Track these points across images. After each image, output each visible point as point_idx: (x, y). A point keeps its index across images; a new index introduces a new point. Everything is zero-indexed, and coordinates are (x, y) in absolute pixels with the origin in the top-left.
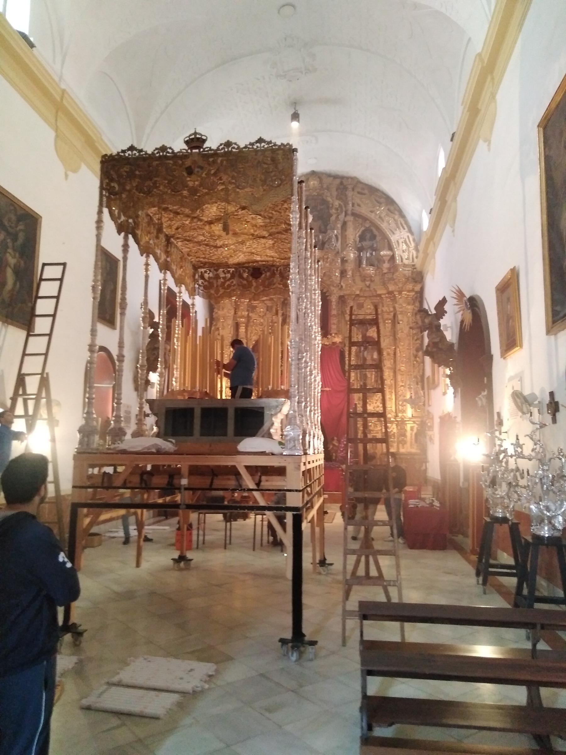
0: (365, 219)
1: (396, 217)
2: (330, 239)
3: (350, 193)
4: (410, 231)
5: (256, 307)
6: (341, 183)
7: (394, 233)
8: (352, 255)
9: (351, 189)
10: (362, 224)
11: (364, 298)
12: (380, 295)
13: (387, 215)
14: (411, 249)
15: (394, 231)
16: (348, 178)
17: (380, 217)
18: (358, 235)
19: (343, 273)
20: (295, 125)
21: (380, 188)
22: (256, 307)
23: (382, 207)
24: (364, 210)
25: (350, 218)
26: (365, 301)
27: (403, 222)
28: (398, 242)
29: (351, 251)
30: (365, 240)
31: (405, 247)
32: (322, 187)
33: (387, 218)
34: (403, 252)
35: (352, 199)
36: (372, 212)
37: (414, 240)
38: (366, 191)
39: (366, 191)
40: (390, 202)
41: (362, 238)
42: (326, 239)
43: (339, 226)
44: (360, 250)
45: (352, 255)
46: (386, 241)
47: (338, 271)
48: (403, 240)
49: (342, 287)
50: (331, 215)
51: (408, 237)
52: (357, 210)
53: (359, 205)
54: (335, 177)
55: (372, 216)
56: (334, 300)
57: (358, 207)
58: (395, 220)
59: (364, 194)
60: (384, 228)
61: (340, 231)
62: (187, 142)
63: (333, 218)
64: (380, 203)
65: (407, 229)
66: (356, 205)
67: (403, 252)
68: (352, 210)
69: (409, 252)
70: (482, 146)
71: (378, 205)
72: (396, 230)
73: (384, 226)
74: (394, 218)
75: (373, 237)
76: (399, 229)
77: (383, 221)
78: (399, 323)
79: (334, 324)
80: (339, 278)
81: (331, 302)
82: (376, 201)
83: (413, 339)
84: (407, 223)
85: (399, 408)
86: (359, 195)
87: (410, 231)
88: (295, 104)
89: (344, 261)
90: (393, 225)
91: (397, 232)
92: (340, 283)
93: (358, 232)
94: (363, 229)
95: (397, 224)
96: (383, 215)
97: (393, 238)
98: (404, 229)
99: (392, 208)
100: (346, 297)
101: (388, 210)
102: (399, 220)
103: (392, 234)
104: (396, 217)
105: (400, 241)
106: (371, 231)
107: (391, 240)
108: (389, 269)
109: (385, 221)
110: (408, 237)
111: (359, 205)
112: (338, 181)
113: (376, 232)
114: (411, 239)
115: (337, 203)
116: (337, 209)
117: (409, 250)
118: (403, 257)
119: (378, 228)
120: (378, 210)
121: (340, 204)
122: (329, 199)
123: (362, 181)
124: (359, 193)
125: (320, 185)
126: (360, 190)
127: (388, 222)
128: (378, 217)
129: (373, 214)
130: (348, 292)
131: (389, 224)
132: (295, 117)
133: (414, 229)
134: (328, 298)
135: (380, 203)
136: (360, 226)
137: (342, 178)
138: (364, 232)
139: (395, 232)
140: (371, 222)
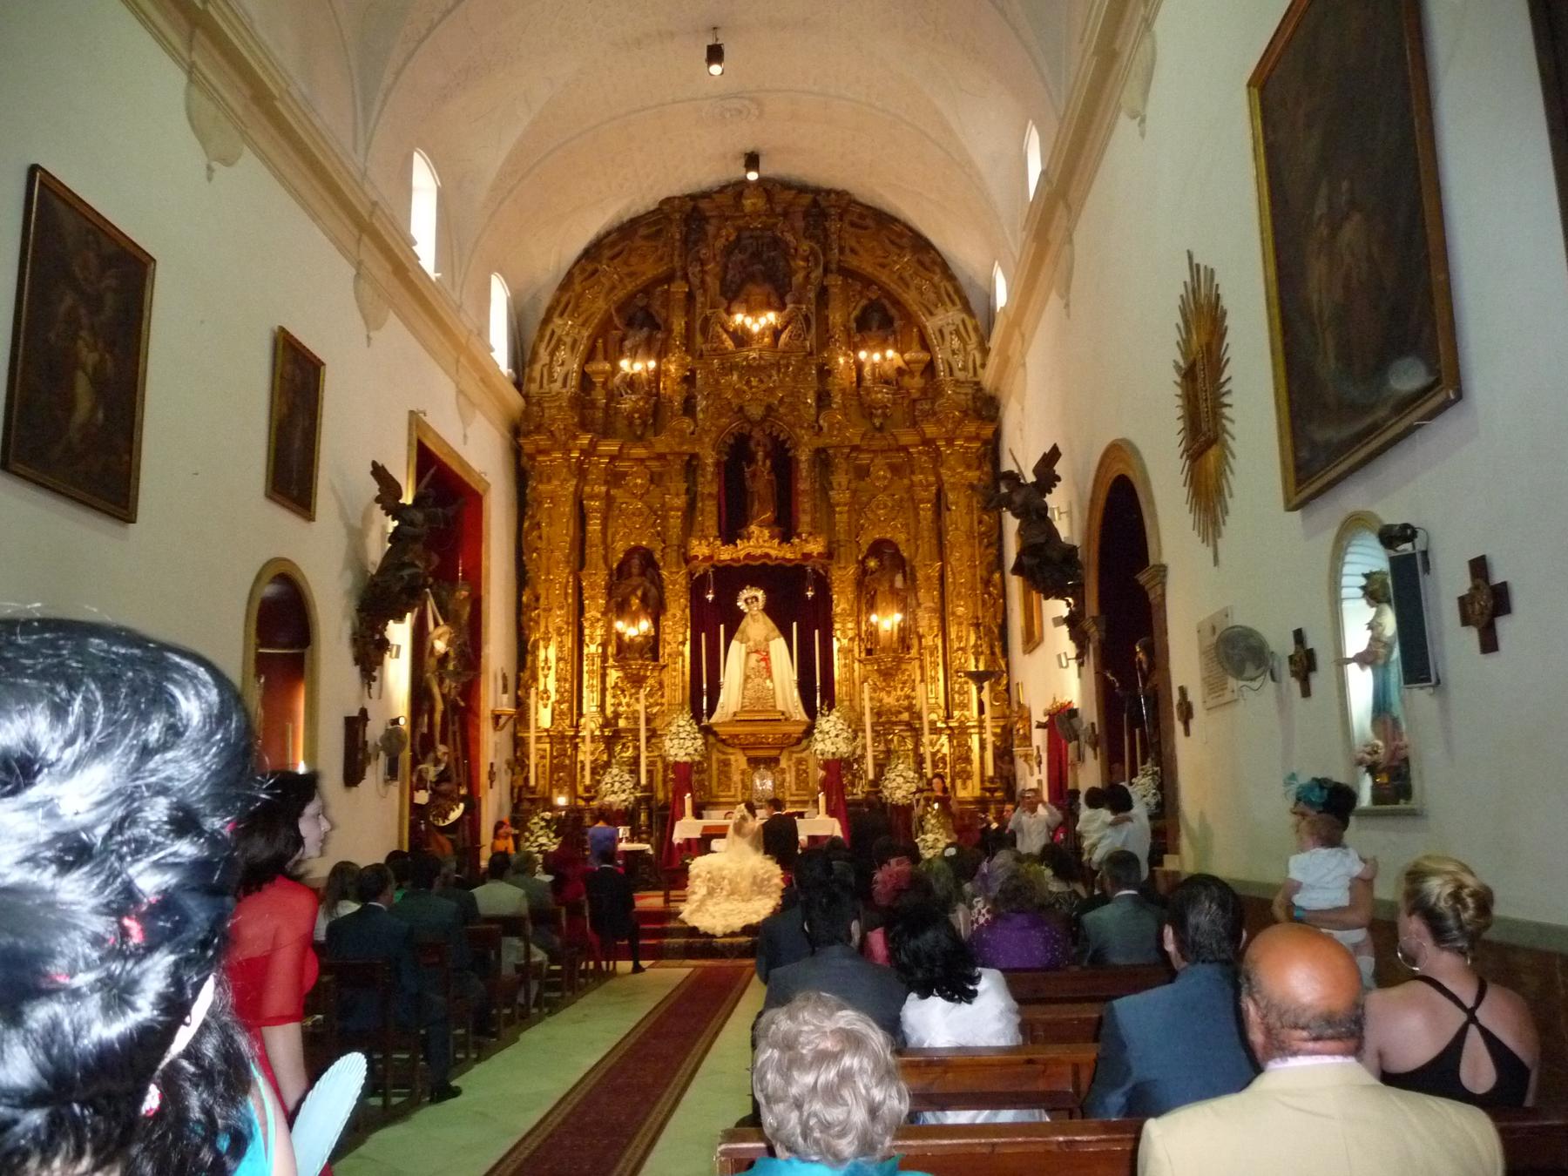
0: (868, 282)
1: (936, 279)
3: (833, 226)
4: (967, 308)
5: (625, 474)
6: (815, 203)
10: (861, 293)
11: (871, 455)
12: (905, 448)
13: (916, 273)
14: (969, 348)
15: (932, 309)
16: (829, 192)
17: (901, 278)
18: (852, 316)
19: (823, 399)
20: (716, 69)
21: (901, 217)
22: (625, 474)
24: (866, 265)
25: (835, 281)
26: (872, 460)
28: (941, 331)
31: (956, 343)
32: (772, 209)
33: (917, 281)
34: (954, 353)
35: (840, 237)
36: (883, 266)
37: (976, 329)
38: (869, 222)
40: (921, 245)
43: (812, 295)
48: (952, 328)
49: (821, 428)
51: (963, 321)
52: (853, 262)
53: (853, 250)
54: (802, 189)
55: (884, 277)
56: (803, 458)
58: (934, 285)
59: (866, 228)
61: (813, 308)
64: (902, 248)
65: (959, 306)
66: (847, 251)
67: (954, 353)
68: (840, 261)
69: (966, 353)
70: (1125, 127)
72: (936, 306)
73: (910, 298)
74: (931, 280)
76: (943, 304)
77: (907, 286)
78: (949, 509)
80: (813, 411)
81: (798, 462)
82: (892, 242)
83: (980, 543)
84: (958, 290)
85: (953, 699)
86: (852, 230)
87: (967, 308)
91: (940, 312)
92: (817, 421)
93: (854, 308)
94: (864, 302)
96: (906, 275)
97: (931, 325)
98: (953, 303)
99: (927, 260)
100: (831, 451)
104: (936, 279)
105: (946, 332)
106: (884, 310)
108: (924, 391)
109: (913, 288)
110: (963, 321)
111: (853, 250)
112: (807, 199)
113: (893, 312)
114: (970, 328)
115: (805, 246)
116: (806, 260)
117: (965, 349)
118: (954, 364)
119: (897, 303)
120: (895, 262)
121: (812, 249)
122: (789, 237)
123: (861, 200)
124: (853, 224)
126: (855, 219)
127: (919, 289)
129: (886, 271)
130: (835, 441)
131: (921, 293)
133: (975, 304)
134: (790, 454)
135: (902, 248)
136: (858, 297)
137: (817, 191)
138: (865, 311)
139: (935, 312)
140: (880, 288)
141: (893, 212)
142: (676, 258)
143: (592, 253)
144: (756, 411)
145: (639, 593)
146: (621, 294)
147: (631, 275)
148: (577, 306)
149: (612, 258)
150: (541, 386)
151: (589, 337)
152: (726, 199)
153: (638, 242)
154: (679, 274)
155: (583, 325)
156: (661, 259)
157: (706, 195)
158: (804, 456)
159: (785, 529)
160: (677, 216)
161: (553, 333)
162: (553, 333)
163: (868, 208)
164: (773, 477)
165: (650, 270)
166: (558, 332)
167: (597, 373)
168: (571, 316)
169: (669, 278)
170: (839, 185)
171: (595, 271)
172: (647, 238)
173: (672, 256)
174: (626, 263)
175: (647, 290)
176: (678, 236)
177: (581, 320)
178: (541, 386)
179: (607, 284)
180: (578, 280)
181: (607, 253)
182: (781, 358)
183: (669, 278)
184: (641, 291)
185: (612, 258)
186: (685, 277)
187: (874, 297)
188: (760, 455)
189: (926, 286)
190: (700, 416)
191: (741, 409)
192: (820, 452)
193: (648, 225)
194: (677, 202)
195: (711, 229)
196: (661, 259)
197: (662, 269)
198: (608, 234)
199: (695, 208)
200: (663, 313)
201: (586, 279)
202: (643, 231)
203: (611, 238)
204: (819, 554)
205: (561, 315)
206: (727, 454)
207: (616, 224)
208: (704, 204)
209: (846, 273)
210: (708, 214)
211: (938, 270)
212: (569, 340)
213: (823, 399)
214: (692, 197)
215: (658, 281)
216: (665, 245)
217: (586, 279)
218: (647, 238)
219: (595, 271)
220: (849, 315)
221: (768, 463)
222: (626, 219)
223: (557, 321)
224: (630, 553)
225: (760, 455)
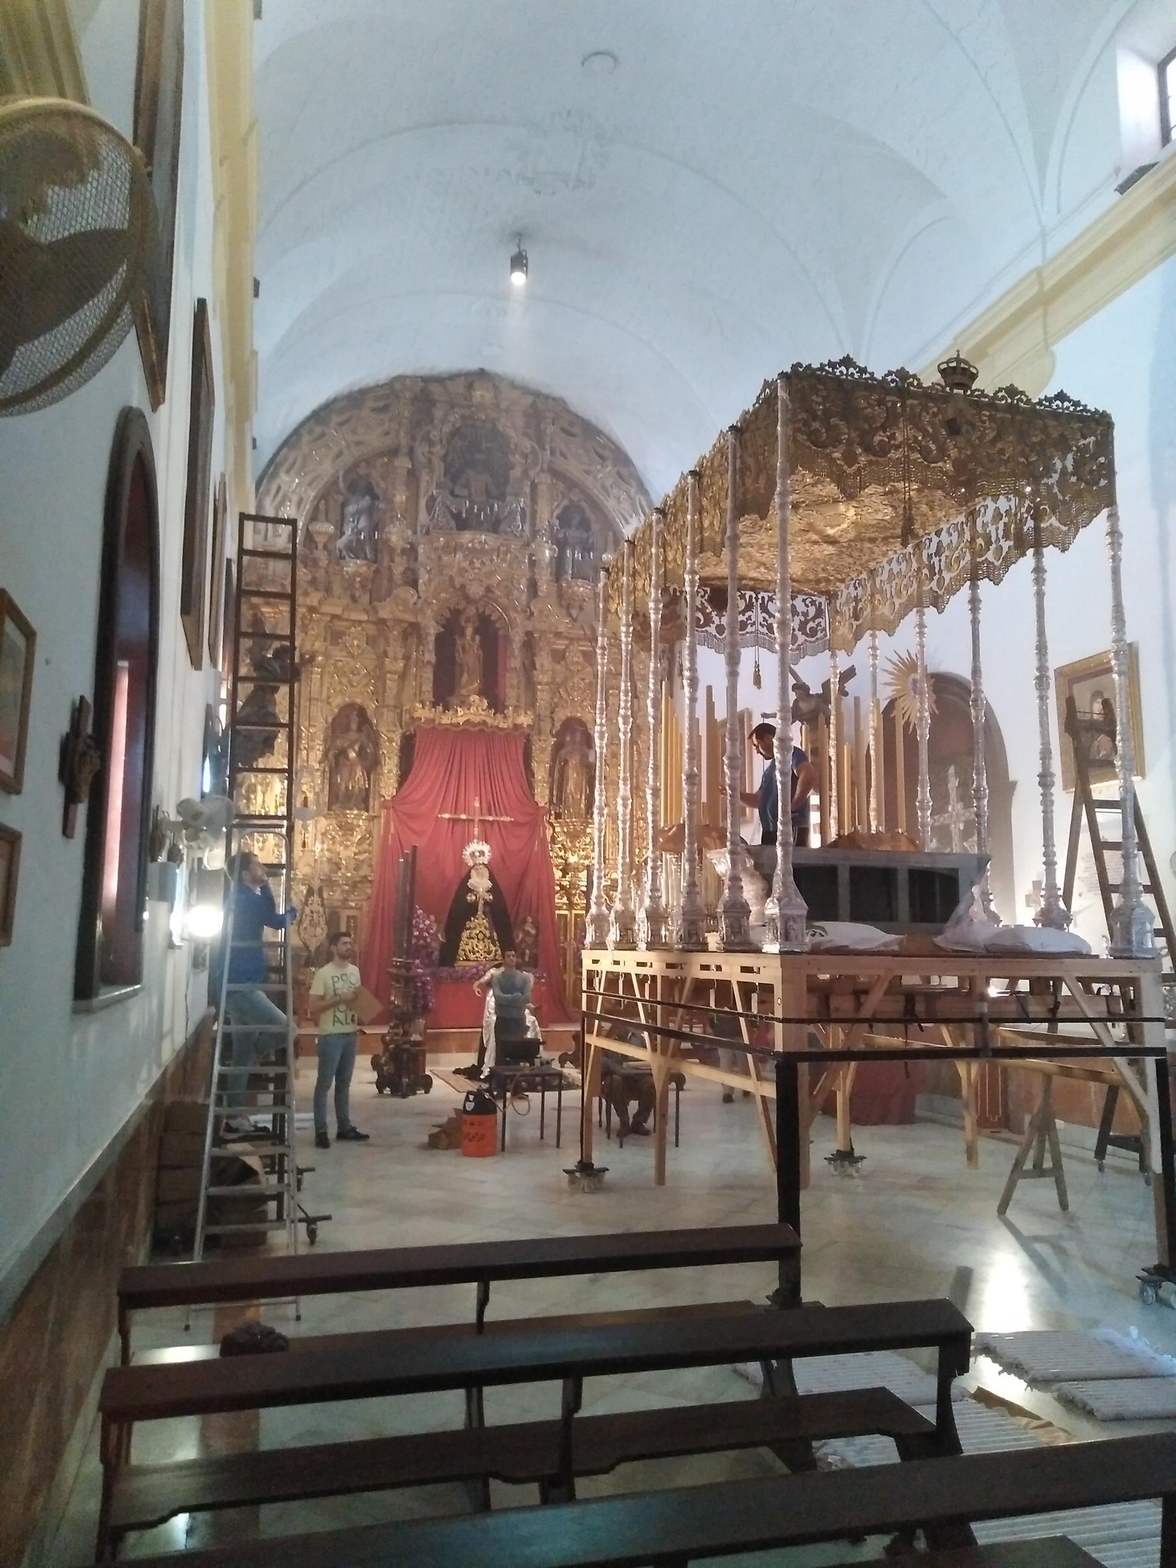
0: (572, 484)
1: (633, 491)
2: (512, 513)
6: (533, 405)
7: (627, 522)
8: (547, 553)
9: (551, 421)
11: (567, 642)
16: (547, 397)
17: (603, 487)
18: (555, 514)
20: (518, 279)
21: (606, 430)
23: (607, 467)
24: (573, 468)
25: (545, 479)
27: (644, 504)
29: (546, 545)
30: (569, 526)
35: (552, 441)
36: (588, 472)
39: (575, 430)
40: (622, 459)
41: (564, 519)
42: (505, 514)
44: (561, 545)
45: (547, 553)
46: (611, 534)
47: (524, 581)
49: (532, 614)
50: (512, 467)
52: (560, 464)
53: (563, 455)
54: (526, 390)
55: (588, 481)
56: (517, 639)
57: (562, 459)
58: (629, 495)
60: (611, 509)
61: (528, 501)
62: (943, 372)
63: (516, 473)
71: (600, 461)
73: (610, 504)
75: (585, 525)
76: (637, 514)
77: (609, 496)
79: (512, 687)
80: (524, 597)
81: (508, 639)
86: (563, 435)
88: (519, 236)
89: (533, 564)
90: (626, 505)
92: (528, 607)
94: (565, 502)
95: (633, 505)
96: (608, 483)
99: (625, 472)
101: (619, 474)
102: (637, 498)
103: (623, 522)
104: (633, 491)
106: (582, 511)
107: (622, 533)
111: (563, 455)
112: (529, 400)
113: (589, 514)
116: (526, 457)
119: (596, 506)
120: (599, 471)
121: (532, 447)
122: (511, 433)
123: (573, 409)
124: (563, 430)
125: (494, 401)
126: (566, 426)
128: (598, 485)
130: (543, 626)
132: (519, 262)
137: (537, 394)
138: (566, 509)
141: (601, 426)
142: (402, 434)
143: (320, 415)
144: (476, 590)
145: (356, 748)
146: (347, 459)
147: (358, 444)
148: (303, 466)
149: (341, 424)
150: (266, 538)
151: (315, 497)
152: (458, 387)
153: (365, 413)
154: (405, 450)
155: (310, 484)
156: (387, 433)
157: (440, 380)
158: (517, 637)
159: (496, 705)
160: (408, 395)
161: (279, 488)
162: (279, 488)
163: (577, 416)
164: (481, 652)
165: (375, 439)
166: (284, 488)
167: (319, 533)
168: (298, 475)
169: (393, 452)
170: (558, 391)
171: (323, 435)
172: (373, 410)
173: (398, 431)
174: (354, 432)
175: (368, 461)
176: (406, 414)
177: (308, 478)
178: (266, 538)
179: (336, 450)
180: (306, 438)
181: (335, 419)
182: (502, 545)
183: (393, 452)
184: (364, 460)
185: (341, 424)
186: (411, 453)
187: (575, 498)
188: (469, 631)
189: (623, 496)
190: (421, 588)
191: (463, 586)
192: (529, 634)
193: (376, 399)
194: (408, 380)
195: (438, 413)
196: (387, 433)
197: (388, 442)
198: (335, 400)
199: (423, 390)
200: (382, 484)
201: (314, 441)
202: (370, 404)
203: (339, 405)
204: (529, 725)
205: (288, 472)
206: (443, 627)
207: (345, 392)
208: (435, 389)
209: (555, 474)
210: (436, 397)
211: (634, 484)
212: (295, 498)
213: (533, 586)
214: (427, 380)
215: (381, 454)
216: (391, 420)
217: (314, 441)
218: (373, 410)
219: (323, 435)
220: (552, 513)
221: (478, 638)
222: (356, 388)
223: (284, 478)
224: (349, 709)
225: (469, 631)
